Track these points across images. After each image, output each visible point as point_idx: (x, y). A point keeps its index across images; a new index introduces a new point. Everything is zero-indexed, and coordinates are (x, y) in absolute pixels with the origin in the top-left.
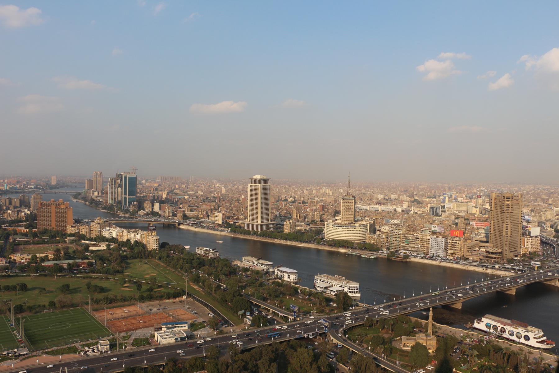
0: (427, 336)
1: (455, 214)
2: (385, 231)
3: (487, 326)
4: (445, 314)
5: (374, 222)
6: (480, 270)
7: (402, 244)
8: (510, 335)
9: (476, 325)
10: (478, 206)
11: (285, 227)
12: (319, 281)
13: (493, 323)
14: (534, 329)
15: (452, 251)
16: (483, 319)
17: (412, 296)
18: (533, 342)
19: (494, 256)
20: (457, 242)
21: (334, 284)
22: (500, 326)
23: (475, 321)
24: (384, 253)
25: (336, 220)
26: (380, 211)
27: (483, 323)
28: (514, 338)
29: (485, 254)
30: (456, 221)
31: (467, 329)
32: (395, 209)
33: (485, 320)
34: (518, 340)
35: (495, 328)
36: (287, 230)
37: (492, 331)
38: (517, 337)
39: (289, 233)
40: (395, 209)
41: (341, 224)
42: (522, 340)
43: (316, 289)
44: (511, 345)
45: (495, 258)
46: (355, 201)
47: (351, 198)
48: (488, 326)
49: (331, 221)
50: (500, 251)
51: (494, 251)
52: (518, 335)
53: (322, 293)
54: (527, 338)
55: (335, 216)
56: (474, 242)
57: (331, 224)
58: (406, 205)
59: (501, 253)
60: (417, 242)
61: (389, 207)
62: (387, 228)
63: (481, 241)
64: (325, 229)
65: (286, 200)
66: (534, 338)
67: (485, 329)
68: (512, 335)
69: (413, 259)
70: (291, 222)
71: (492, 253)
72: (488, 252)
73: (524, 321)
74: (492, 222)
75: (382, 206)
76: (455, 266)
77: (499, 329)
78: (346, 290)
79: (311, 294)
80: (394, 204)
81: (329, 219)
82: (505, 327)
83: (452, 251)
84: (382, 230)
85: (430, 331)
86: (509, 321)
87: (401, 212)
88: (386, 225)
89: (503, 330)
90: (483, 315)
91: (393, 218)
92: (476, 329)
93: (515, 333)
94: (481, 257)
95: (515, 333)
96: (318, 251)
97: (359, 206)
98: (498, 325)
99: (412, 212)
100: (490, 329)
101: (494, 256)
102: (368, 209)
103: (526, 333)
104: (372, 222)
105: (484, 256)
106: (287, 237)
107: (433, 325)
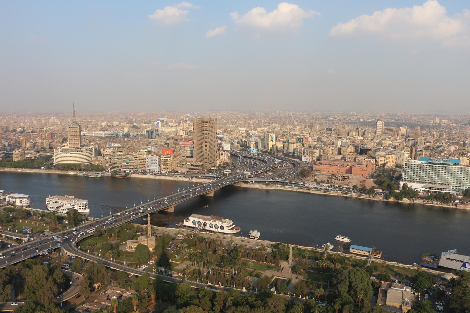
0: (147, 237)
1: (166, 136)
2: (108, 153)
3: (193, 223)
4: (161, 218)
5: (98, 146)
6: (187, 179)
7: (123, 164)
9: (186, 223)
10: (185, 129)
11: (14, 156)
12: (50, 203)
14: (227, 220)
15: (165, 167)
16: (190, 218)
17: (148, 202)
18: (226, 230)
19: (197, 168)
21: (65, 203)
22: (203, 221)
23: (185, 220)
24: (108, 173)
25: (64, 146)
26: (104, 136)
28: (214, 229)
29: (190, 167)
30: (168, 142)
31: (178, 227)
33: (192, 219)
35: (200, 223)
36: (16, 158)
37: (197, 226)
38: (216, 228)
39: (19, 161)
41: (68, 150)
42: (219, 230)
43: (48, 209)
44: (211, 235)
45: (198, 169)
46: (80, 129)
47: (77, 126)
48: (194, 223)
49: (59, 147)
50: (201, 163)
51: (197, 164)
52: (216, 226)
53: (54, 212)
54: (222, 228)
55: (63, 142)
56: (182, 158)
57: (60, 150)
59: (203, 165)
60: (136, 161)
62: (110, 151)
63: (187, 157)
64: (54, 155)
65: (15, 130)
66: (227, 227)
67: (192, 225)
68: (211, 227)
70: (20, 150)
71: (196, 166)
73: (219, 216)
75: (106, 132)
76: (168, 178)
78: (76, 207)
79: (43, 215)
81: (58, 146)
82: (206, 222)
83: (165, 167)
84: (106, 153)
85: (149, 233)
86: (209, 217)
87: (122, 136)
88: (109, 148)
89: (205, 225)
90: (190, 215)
92: (185, 226)
96: (49, 175)
97: (86, 133)
100: (195, 225)
101: (197, 168)
102: (94, 135)
103: (222, 224)
104: (97, 146)
105: (189, 169)
106: (18, 165)
107: (151, 228)
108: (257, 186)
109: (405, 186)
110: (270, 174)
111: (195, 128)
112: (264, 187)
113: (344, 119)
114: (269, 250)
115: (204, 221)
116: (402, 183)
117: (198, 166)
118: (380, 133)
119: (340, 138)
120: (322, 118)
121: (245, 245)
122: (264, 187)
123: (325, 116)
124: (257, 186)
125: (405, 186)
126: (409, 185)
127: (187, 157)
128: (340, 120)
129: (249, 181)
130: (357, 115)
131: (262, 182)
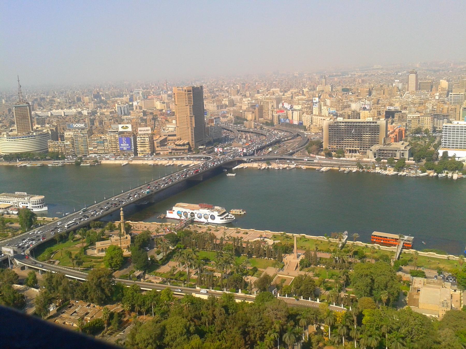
6: (171, 163)
7: (89, 148)
8: (199, 217)
13: (184, 210)
15: (142, 149)
18: (218, 220)
19: (183, 148)
20: (146, 139)
24: (70, 160)
26: (63, 115)
27: (177, 212)
28: (203, 220)
32: (80, 113)
34: (205, 221)
40: (80, 113)
42: (210, 220)
44: (200, 227)
45: (183, 150)
50: (186, 142)
51: (181, 144)
52: (206, 216)
54: (213, 217)
56: (163, 138)
58: (91, 106)
59: (188, 144)
61: (73, 111)
63: (169, 136)
66: (218, 216)
67: (178, 217)
69: (104, 162)
71: (180, 145)
72: (177, 145)
74: (177, 115)
75: (65, 110)
77: (189, 214)
80: (79, 107)
83: (142, 149)
86: (197, 206)
87: (87, 114)
88: (70, 130)
91: (78, 122)
93: (203, 215)
94: (170, 151)
95: (203, 215)
97: (39, 112)
98: (188, 211)
99: (98, 114)
101: (183, 148)
102: (50, 115)
103: (212, 213)
105: (173, 149)
108: (255, 165)
109: (445, 154)
110: (270, 149)
111: (176, 99)
112: (264, 166)
113: (366, 75)
114: (270, 242)
115: (191, 211)
116: (441, 152)
117: (184, 145)
118: (414, 89)
119: (360, 99)
120: (336, 76)
121: (242, 238)
122: (264, 166)
123: (339, 74)
124: (255, 165)
125: (445, 154)
126: (451, 153)
127: (169, 136)
128: (360, 76)
129: (245, 159)
130: (382, 69)
131: (260, 160)
